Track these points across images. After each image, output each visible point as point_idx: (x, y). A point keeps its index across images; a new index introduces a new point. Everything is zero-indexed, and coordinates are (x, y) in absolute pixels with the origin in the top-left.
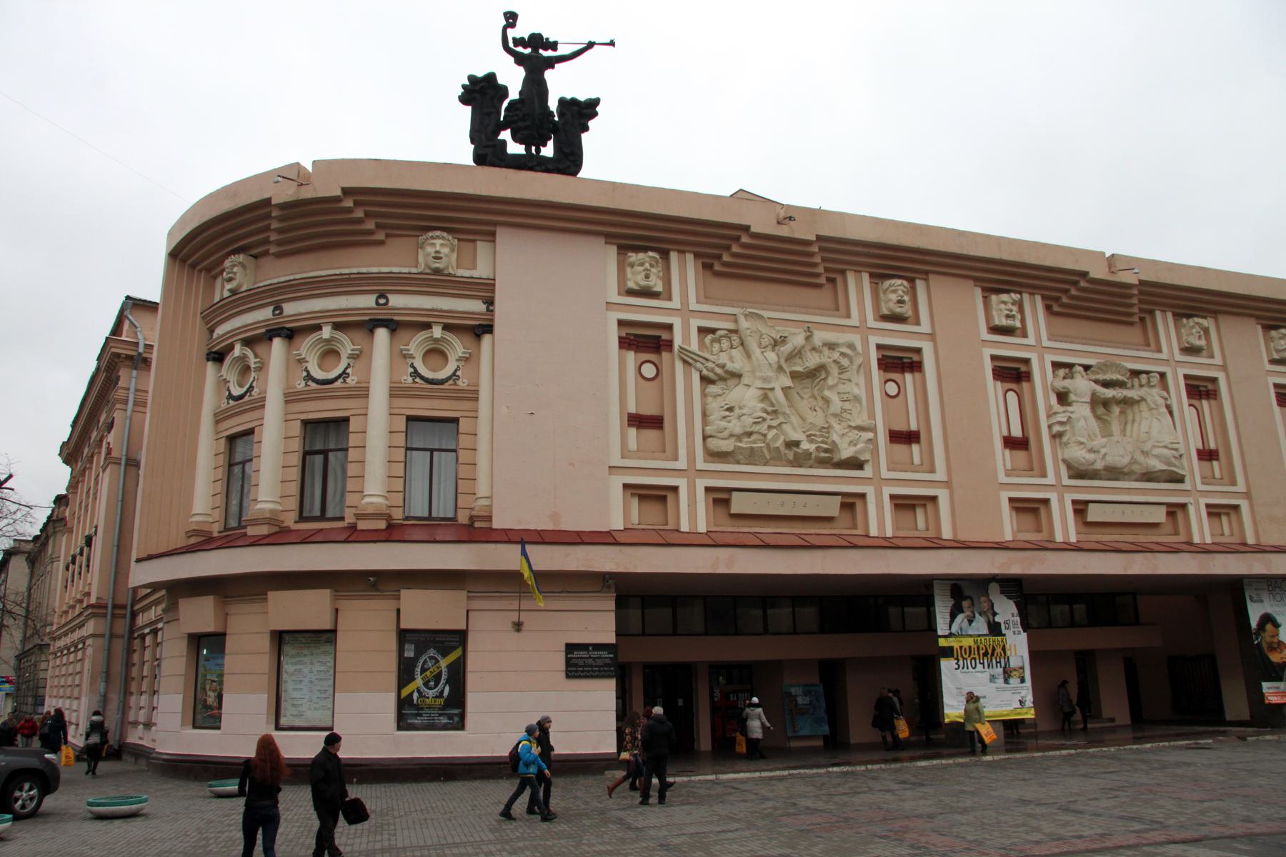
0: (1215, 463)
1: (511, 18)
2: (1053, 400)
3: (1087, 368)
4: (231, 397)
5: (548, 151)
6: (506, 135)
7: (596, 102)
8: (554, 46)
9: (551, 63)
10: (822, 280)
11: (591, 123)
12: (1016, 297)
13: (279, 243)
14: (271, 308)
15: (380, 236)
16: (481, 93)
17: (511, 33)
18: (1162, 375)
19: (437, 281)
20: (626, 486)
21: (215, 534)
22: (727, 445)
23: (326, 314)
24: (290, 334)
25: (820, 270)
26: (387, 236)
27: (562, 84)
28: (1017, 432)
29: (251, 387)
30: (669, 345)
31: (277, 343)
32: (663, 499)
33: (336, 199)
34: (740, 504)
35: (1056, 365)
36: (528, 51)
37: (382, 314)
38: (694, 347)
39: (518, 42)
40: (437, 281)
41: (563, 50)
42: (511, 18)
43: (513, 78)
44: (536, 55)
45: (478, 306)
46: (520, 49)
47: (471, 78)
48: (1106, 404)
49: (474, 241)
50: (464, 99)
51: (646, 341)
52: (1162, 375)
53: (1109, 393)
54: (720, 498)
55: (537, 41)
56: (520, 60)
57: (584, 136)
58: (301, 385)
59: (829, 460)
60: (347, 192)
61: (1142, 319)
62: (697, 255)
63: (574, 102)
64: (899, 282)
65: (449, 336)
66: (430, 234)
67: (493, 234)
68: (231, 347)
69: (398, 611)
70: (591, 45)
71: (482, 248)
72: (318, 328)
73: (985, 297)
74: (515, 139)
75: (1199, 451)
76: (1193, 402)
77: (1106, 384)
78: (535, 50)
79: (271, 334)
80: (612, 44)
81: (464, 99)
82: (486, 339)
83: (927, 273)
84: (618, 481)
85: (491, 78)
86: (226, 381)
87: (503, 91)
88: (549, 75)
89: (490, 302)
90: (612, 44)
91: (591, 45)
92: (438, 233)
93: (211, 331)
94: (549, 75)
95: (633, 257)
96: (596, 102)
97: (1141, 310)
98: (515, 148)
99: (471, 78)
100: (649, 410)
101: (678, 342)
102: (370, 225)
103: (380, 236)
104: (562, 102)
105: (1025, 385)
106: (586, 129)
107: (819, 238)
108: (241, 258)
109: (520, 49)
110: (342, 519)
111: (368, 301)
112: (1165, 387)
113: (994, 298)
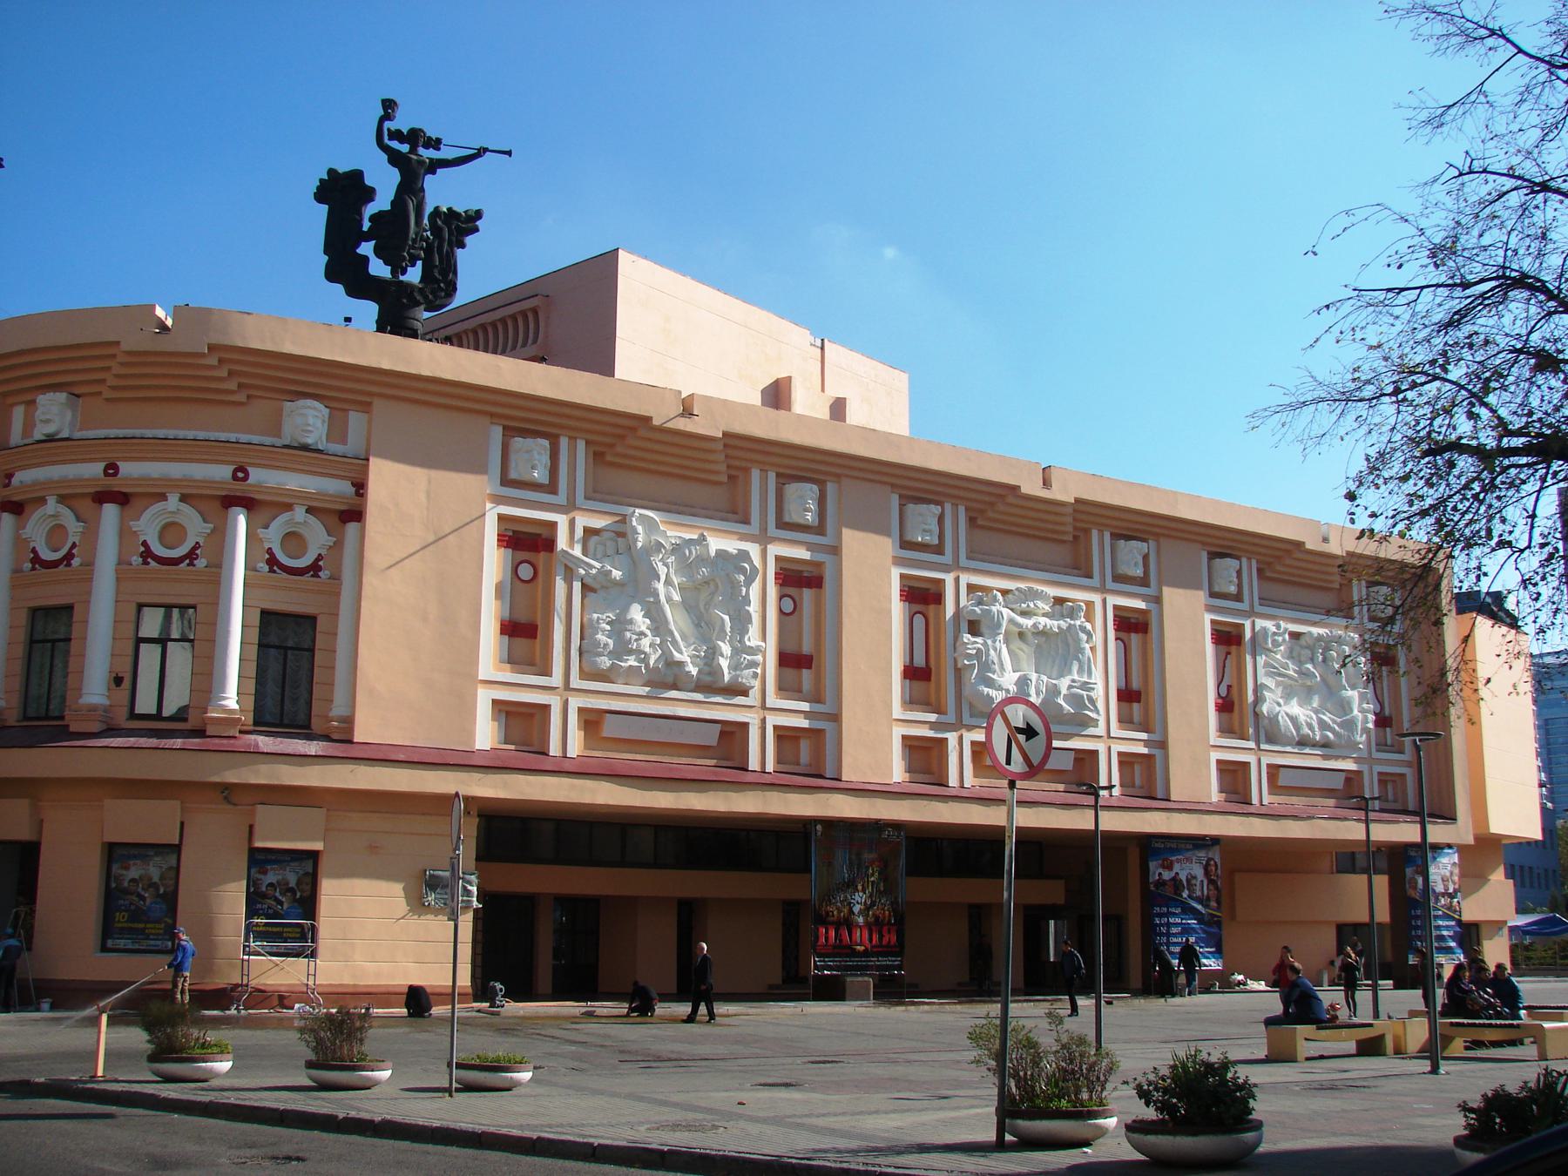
0: (1135, 705)
1: (389, 106)
2: (964, 626)
3: (1005, 592)
4: (36, 560)
5: (414, 275)
6: (366, 249)
7: (478, 215)
8: (436, 144)
9: (434, 166)
10: (724, 479)
11: (469, 240)
12: (937, 510)
13: (114, 388)
14: (102, 465)
15: (241, 397)
16: (342, 191)
17: (387, 125)
18: (1090, 604)
19: (303, 453)
20: (495, 702)
21: (12, 722)
22: (605, 662)
23: (173, 484)
24: (122, 499)
25: (723, 468)
26: (249, 397)
27: (441, 192)
28: (919, 661)
29: (69, 557)
30: (549, 544)
31: (110, 511)
32: (532, 715)
33: (202, 355)
34: (610, 728)
35: (971, 588)
36: (405, 148)
37: (238, 489)
38: (577, 551)
39: (397, 135)
40: (303, 453)
41: (446, 153)
42: (389, 106)
43: (384, 182)
44: (413, 155)
45: (346, 488)
46: (395, 144)
47: (331, 172)
48: (1021, 635)
49: (347, 410)
50: (322, 195)
51: (528, 544)
52: (1090, 604)
53: (1027, 623)
54: (592, 721)
55: (414, 137)
56: (395, 158)
57: (459, 252)
58: (137, 560)
59: (710, 685)
60: (212, 348)
61: (1075, 537)
62: (587, 443)
63: (452, 213)
64: (809, 486)
65: (312, 519)
66: (302, 402)
67: (369, 404)
68: (42, 501)
69: (251, 827)
70: (481, 152)
71: (355, 419)
72: (162, 497)
73: (902, 506)
74: (378, 252)
75: (1119, 692)
76: (1122, 635)
77: (1024, 614)
78: (413, 150)
79: (101, 497)
80: (509, 153)
81: (322, 195)
82: (352, 527)
83: (838, 476)
84: (484, 699)
85: (357, 175)
86: (26, 541)
87: (369, 194)
88: (430, 182)
89: (360, 487)
90: (509, 153)
91: (481, 152)
92: (309, 402)
93: (10, 476)
94: (430, 182)
95: (518, 442)
96: (478, 215)
97: (1075, 528)
98: (379, 269)
99: (331, 172)
100: (523, 617)
101: (562, 543)
102: (232, 385)
103: (241, 397)
104: (437, 212)
105: (932, 608)
106: (463, 246)
107: (725, 434)
108: (62, 396)
109: (395, 144)
110: (186, 720)
111: (223, 472)
112: (1089, 617)
113: (911, 506)
